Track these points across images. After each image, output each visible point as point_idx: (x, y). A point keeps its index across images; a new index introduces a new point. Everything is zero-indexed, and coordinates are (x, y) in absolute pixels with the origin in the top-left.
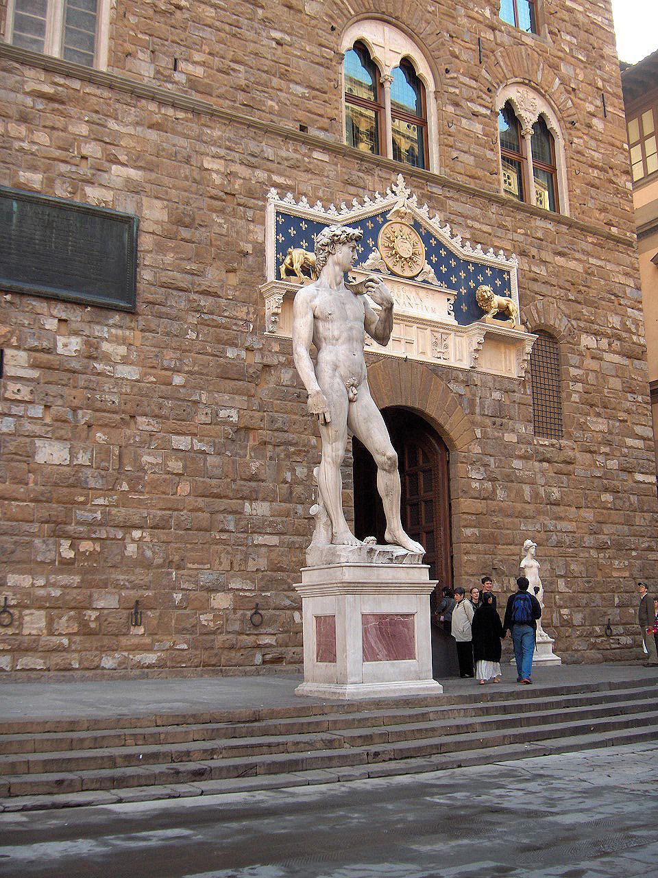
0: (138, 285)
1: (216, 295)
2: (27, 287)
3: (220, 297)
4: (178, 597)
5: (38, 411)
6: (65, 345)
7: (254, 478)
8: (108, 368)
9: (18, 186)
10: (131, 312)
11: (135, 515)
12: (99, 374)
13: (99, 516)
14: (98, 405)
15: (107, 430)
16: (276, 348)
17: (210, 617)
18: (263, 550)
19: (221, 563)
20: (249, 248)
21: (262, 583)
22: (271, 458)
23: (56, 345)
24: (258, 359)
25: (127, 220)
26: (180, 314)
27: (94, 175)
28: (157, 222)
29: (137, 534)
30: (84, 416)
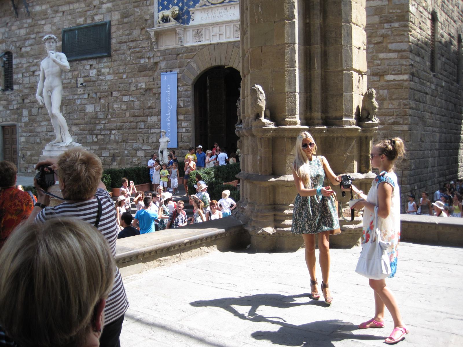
0: (111, 46)
1: (136, 40)
2: (79, 58)
3: (138, 41)
4: (126, 152)
5: (86, 96)
6: (92, 73)
7: (150, 108)
8: (104, 77)
9: (78, 25)
10: (109, 55)
11: (112, 125)
12: (101, 80)
13: (102, 127)
14: (101, 91)
15: (104, 98)
16: (159, 54)
17: (136, 159)
18: (155, 135)
19: (139, 140)
20: (148, 17)
21: (154, 147)
22: (157, 99)
23: (89, 74)
24: (152, 61)
25: (105, 24)
26: (125, 52)
27: (97, 12)
28: (116, 20)
29: (113, 132)
30: (99, 95)
